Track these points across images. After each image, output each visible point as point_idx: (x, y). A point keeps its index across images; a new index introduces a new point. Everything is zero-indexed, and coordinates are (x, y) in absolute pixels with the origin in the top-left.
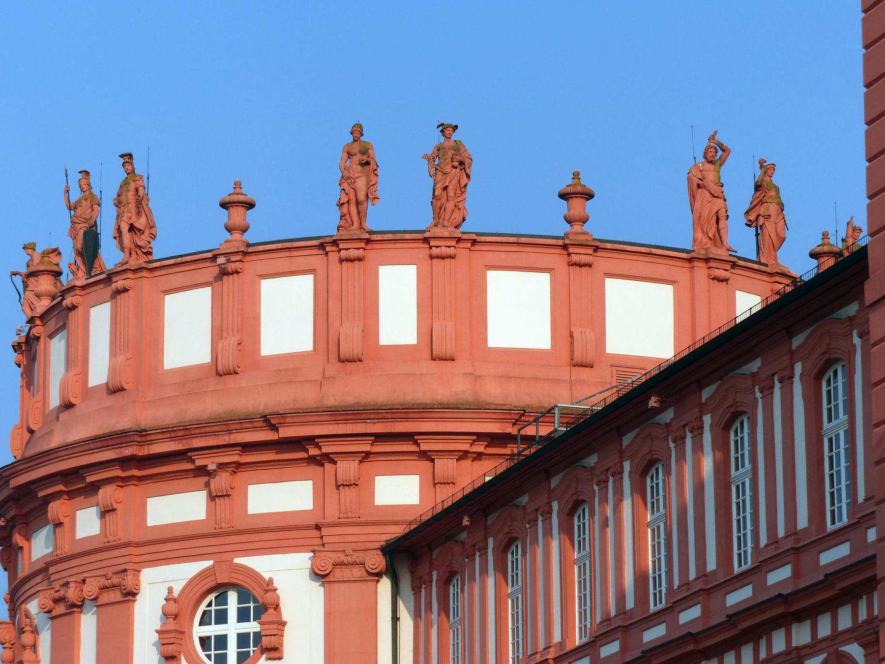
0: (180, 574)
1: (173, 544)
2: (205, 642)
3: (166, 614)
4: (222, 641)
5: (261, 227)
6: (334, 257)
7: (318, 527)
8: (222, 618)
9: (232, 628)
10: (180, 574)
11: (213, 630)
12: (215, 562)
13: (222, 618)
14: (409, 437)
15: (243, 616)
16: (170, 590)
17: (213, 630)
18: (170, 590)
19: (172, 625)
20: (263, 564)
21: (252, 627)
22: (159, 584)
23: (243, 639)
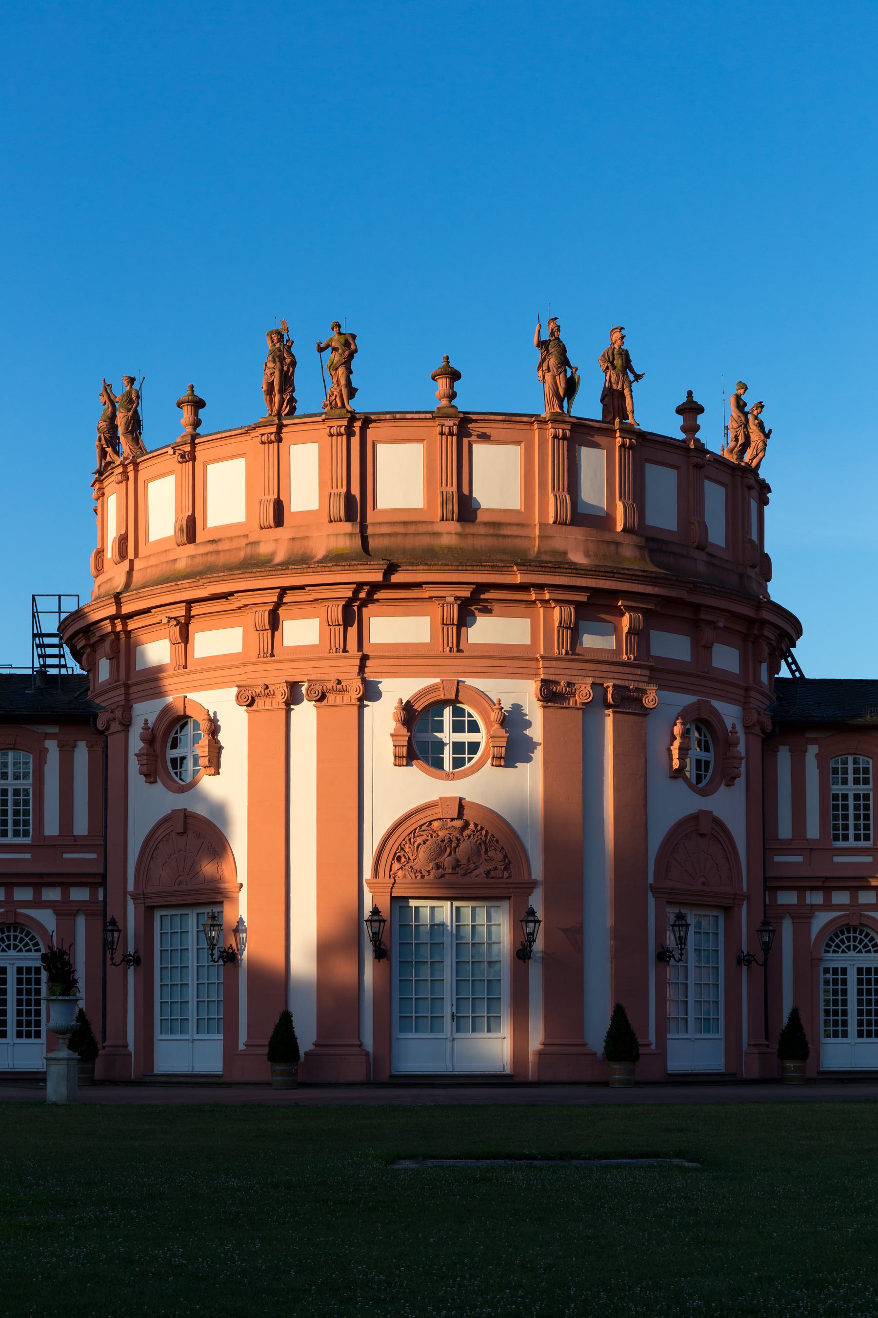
12: (442, 681)
15: (458, 727)
21: (466, 737)
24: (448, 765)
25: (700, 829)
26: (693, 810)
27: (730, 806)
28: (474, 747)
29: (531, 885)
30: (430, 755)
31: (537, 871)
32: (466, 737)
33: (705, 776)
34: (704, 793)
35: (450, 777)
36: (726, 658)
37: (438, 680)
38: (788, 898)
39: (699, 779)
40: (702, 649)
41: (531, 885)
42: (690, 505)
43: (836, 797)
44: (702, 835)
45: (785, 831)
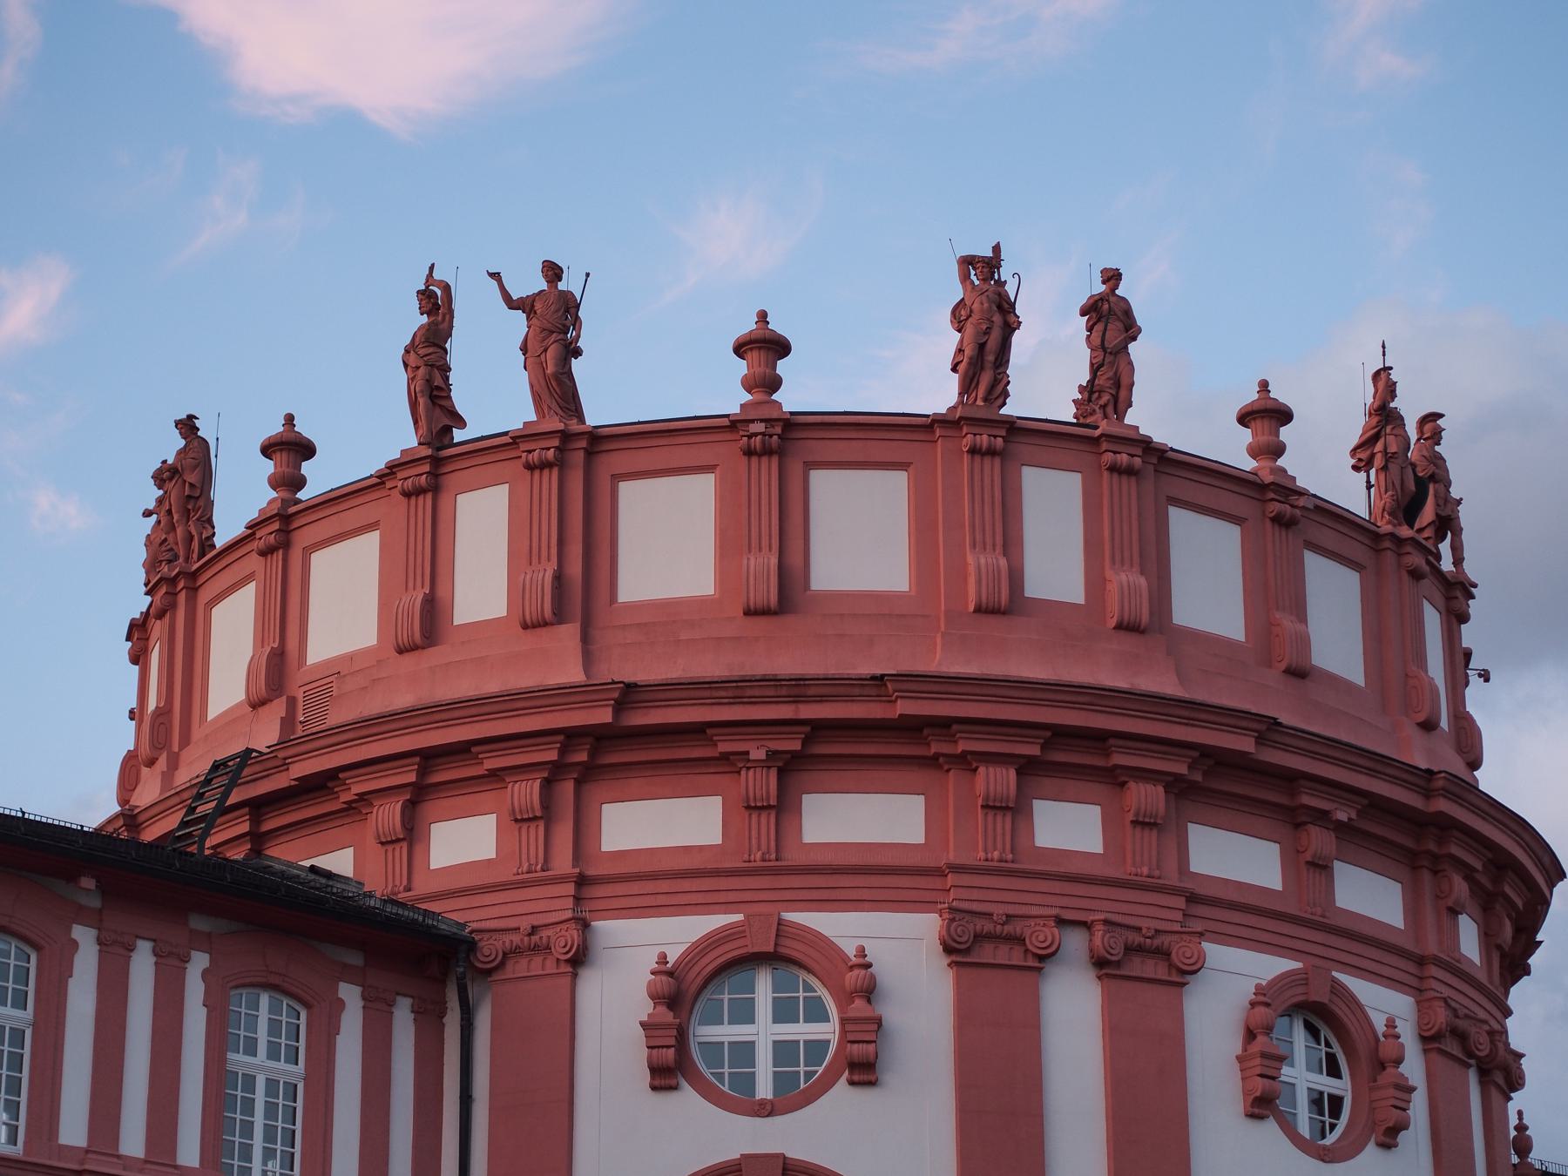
1: (663, 882)
3: (655, 997)
4: (745, 1051)
5: (803, 390)
8: (745, 1014)
9: (764, 1032)
10: (678, 933)
11: (726, 1032)
12: (747, 917)
13: (745, 1014)
14: (1099, 739)
15: (784, 1012)
16: (663, 959)
17: (726, 1032)
18: (663, 959)
20: (842, 928)
21: (802, 1031)
22: (636, 950)
24: (764, 1089)
28: (816, 1048)
30: (726, 1070)
32: (802, 1031)
33: (1333, 1127)
36: (1369, 895)
37: (739, 917)
40: (1310, 870)
42: (1275, 595)
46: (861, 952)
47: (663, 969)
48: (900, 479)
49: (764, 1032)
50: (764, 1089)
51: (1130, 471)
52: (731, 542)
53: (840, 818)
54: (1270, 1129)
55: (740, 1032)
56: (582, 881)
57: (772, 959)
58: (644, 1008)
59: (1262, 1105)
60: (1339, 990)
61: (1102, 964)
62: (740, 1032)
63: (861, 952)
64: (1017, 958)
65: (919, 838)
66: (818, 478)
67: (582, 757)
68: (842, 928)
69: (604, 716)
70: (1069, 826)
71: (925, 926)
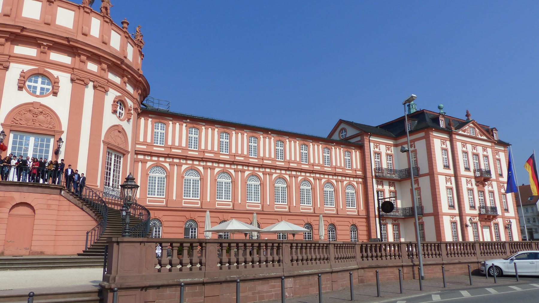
0: (27, 68)
2: (30, 87)
3: (21, 76)
4: (35, 88)
6: (82, 9)
7: (73, 69)
8: (36, 82)
9: (39, 85)
10: (27, 68)
11: (32, 84)
13: (36, 82)
15: (43, 83)
16: (23, 71)
17: (32, 84)
18: (23, 71)
19: (22, 79)
20: (55, 73)
21: (46, 86)
23: (42, 89)
24: (38, 93)
25: (117, 129)
26: (117, 124)
27: (128, 127)
29: (63, 132)
31: (65, 128)
32: (46, 86)
34: (121, 120)
35: (38, 96)
36: (129, 88)
38: (141, 157)
39: (119, 117)
41: (63, 132)
43: (155, 132)
44: (119, 132)
45: (141, 139)
46: (58, 77)
47: (23, 72)
48: (73, 13)
49: (39, 85)
50: (38, 93)
51: (107, 22)
52: (43, 12)
53: (55, 57)
54: (114, 116)
55: (35, 85)
56: (10, 56)
57: (43, 75)
58: (18, 77)
59: (115, 112)
60: (125, 99)
61: (95, 87)
62: (35, 85)
63: (58, 77)
64: (83, 83)
65: (70, 63)
66: (59, 8)
67: (13, 37)
68: (55, 73)
69: (19, 31)
70: (92, 67)
71: (68, 76)
